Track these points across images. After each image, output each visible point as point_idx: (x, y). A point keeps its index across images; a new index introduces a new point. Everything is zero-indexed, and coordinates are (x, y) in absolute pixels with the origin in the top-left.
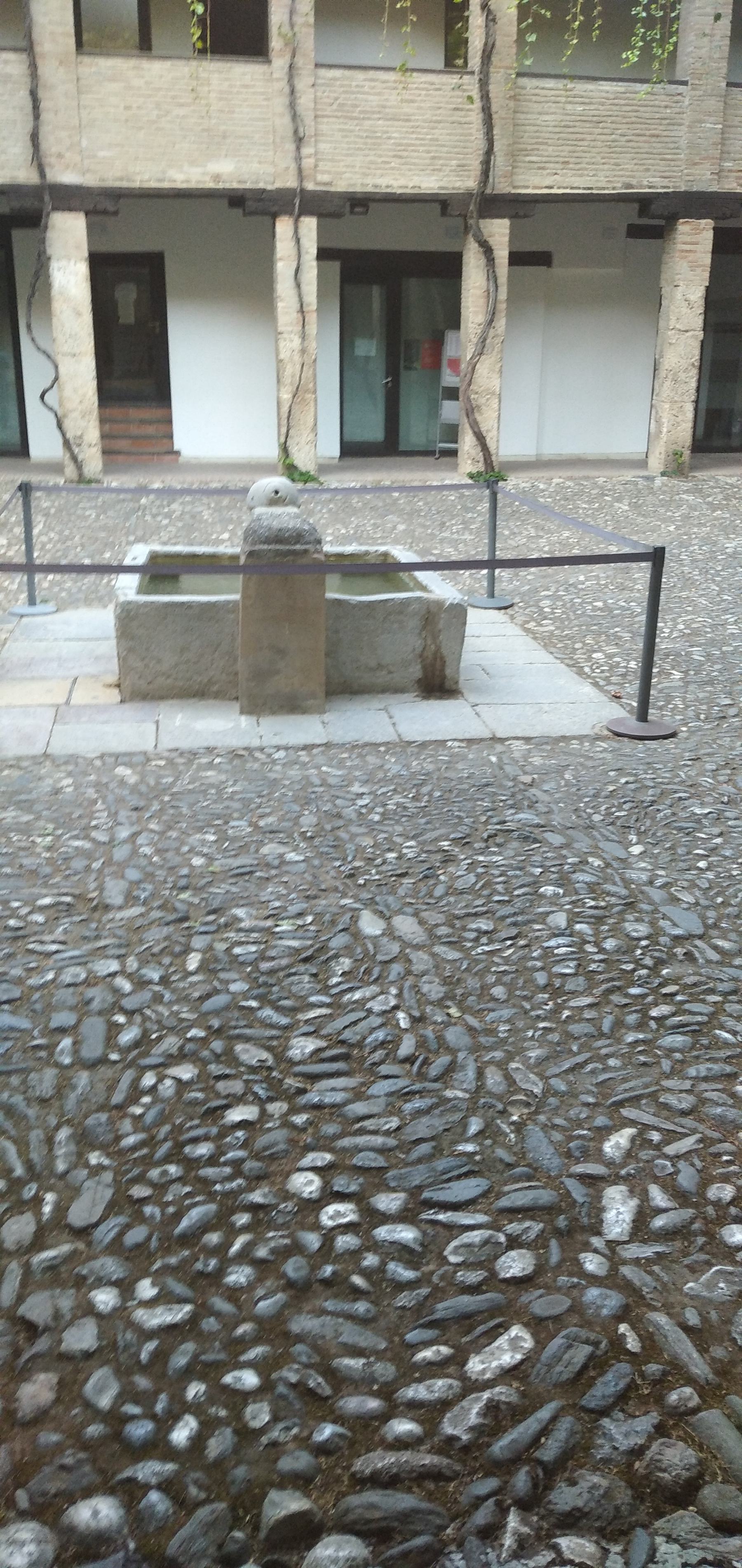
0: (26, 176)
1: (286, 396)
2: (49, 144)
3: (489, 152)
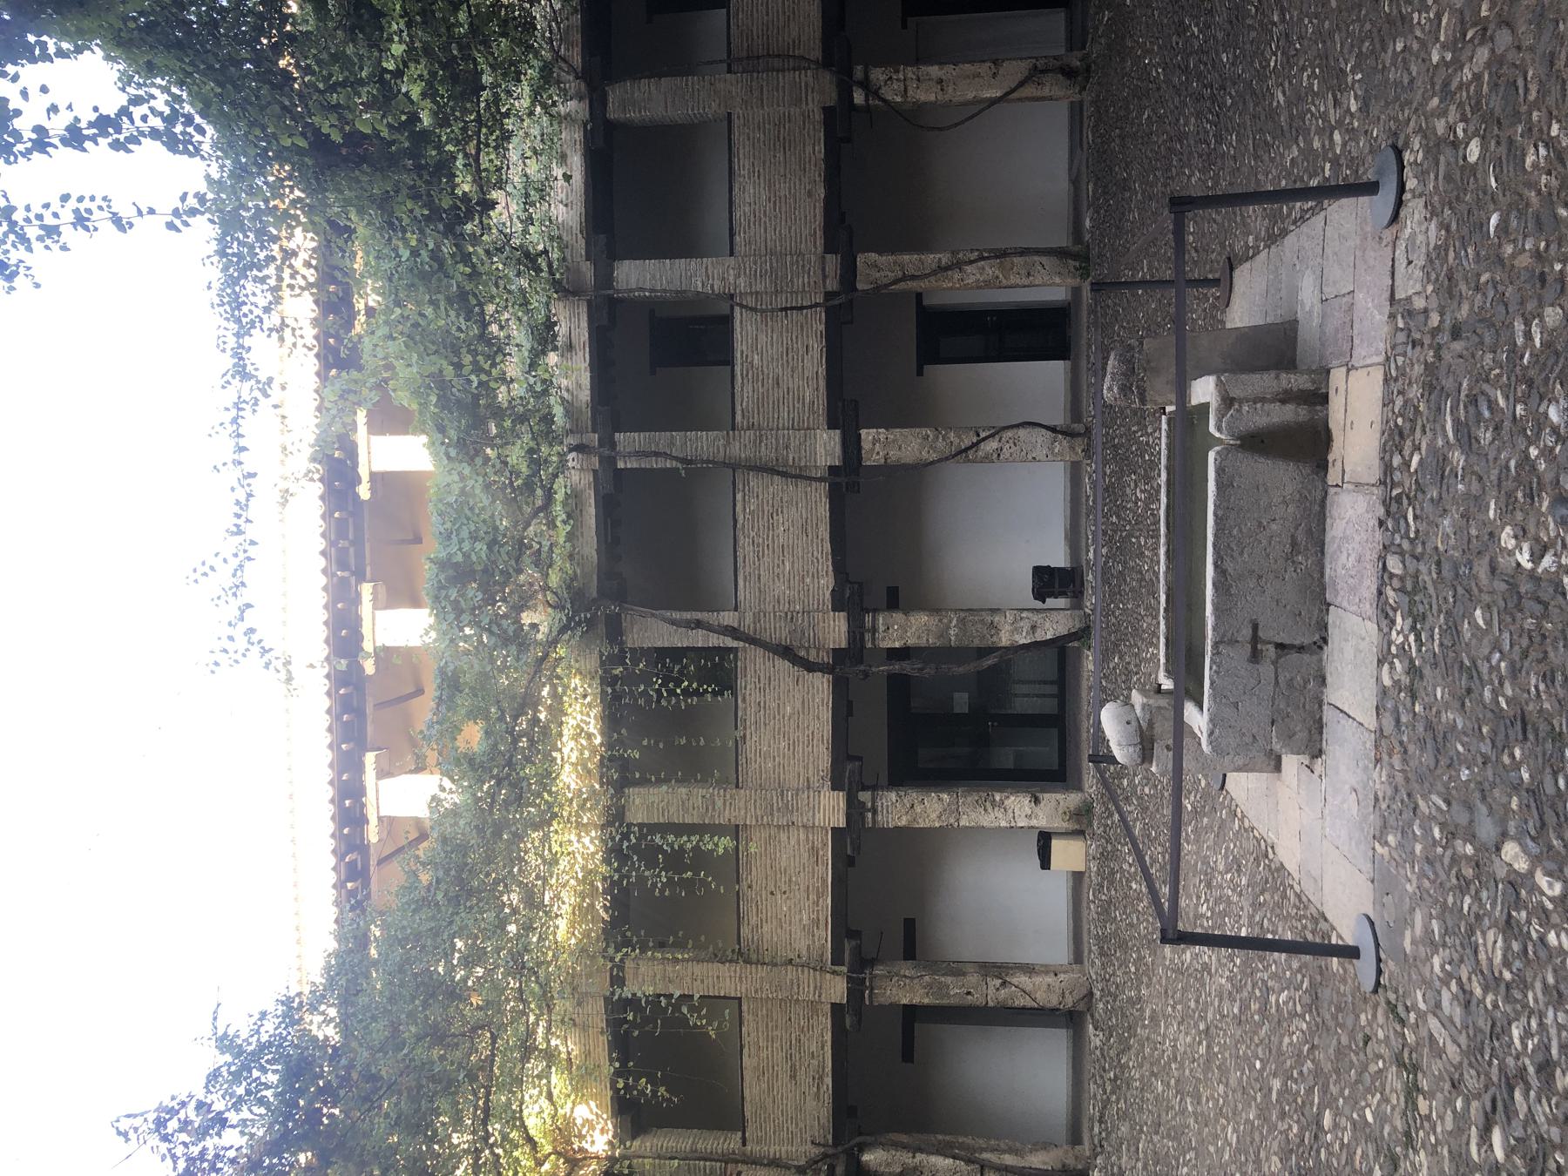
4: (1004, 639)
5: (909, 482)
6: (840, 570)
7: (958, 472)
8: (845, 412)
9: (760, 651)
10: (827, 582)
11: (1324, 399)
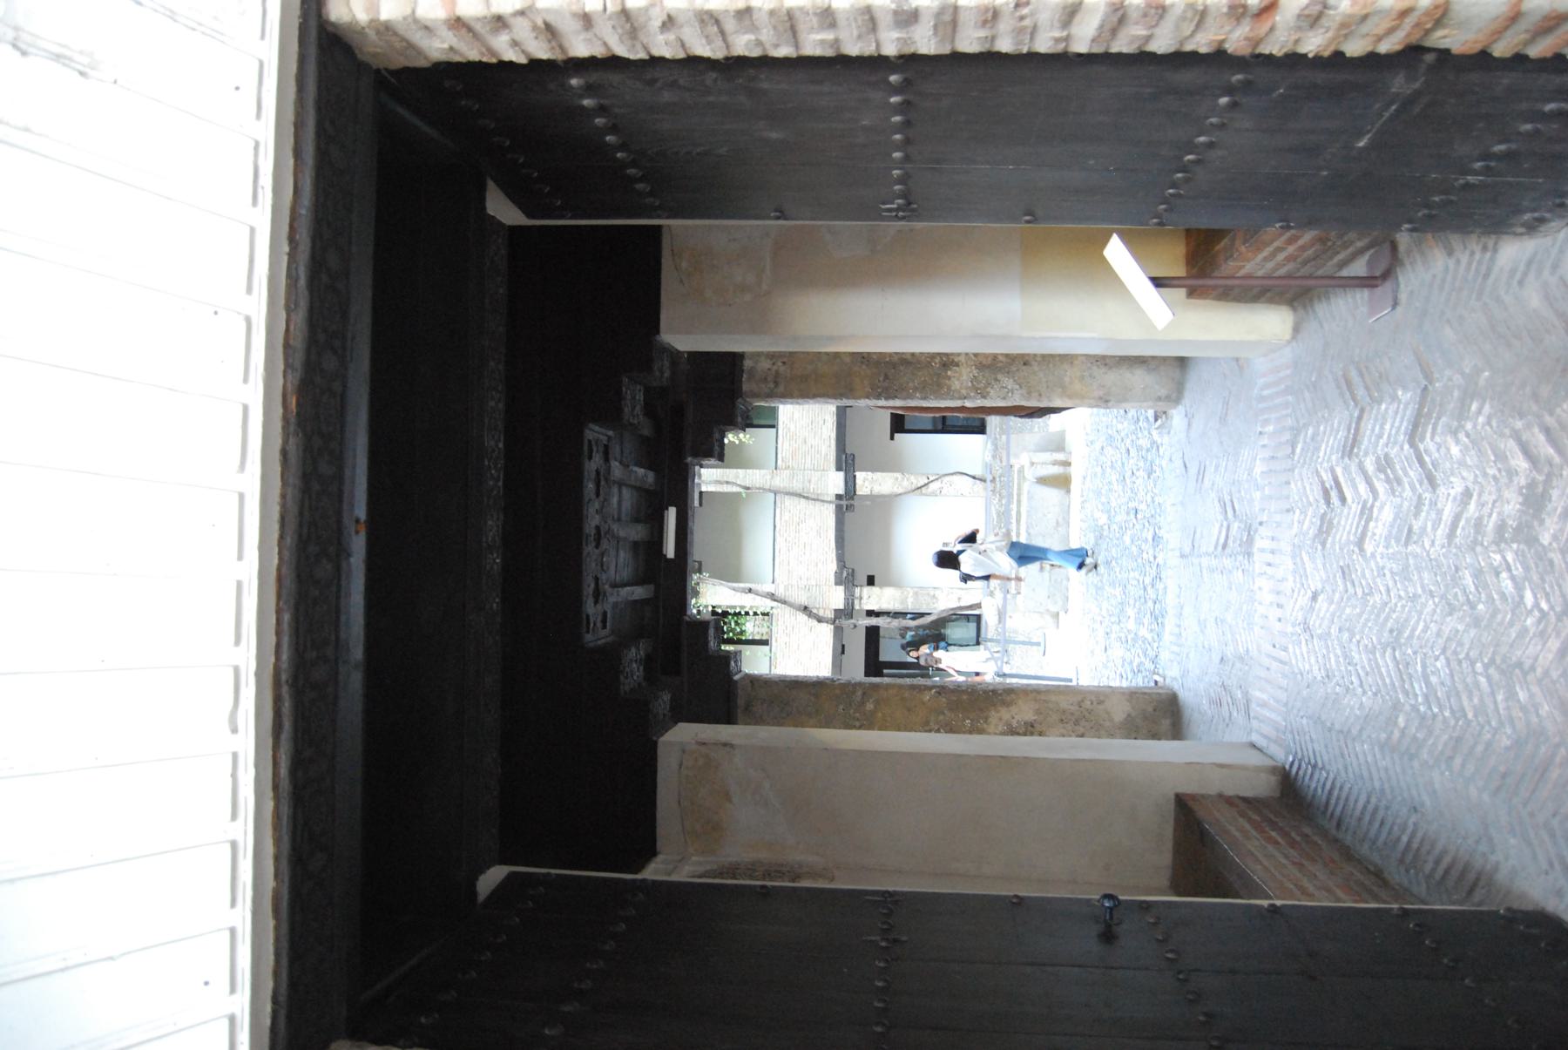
5: (884, 504)
6: (841, 559)
7: (915, 502)
8: (846, 462)
9: (787, 609)
10: (833, 566)
11: (1069, 464)
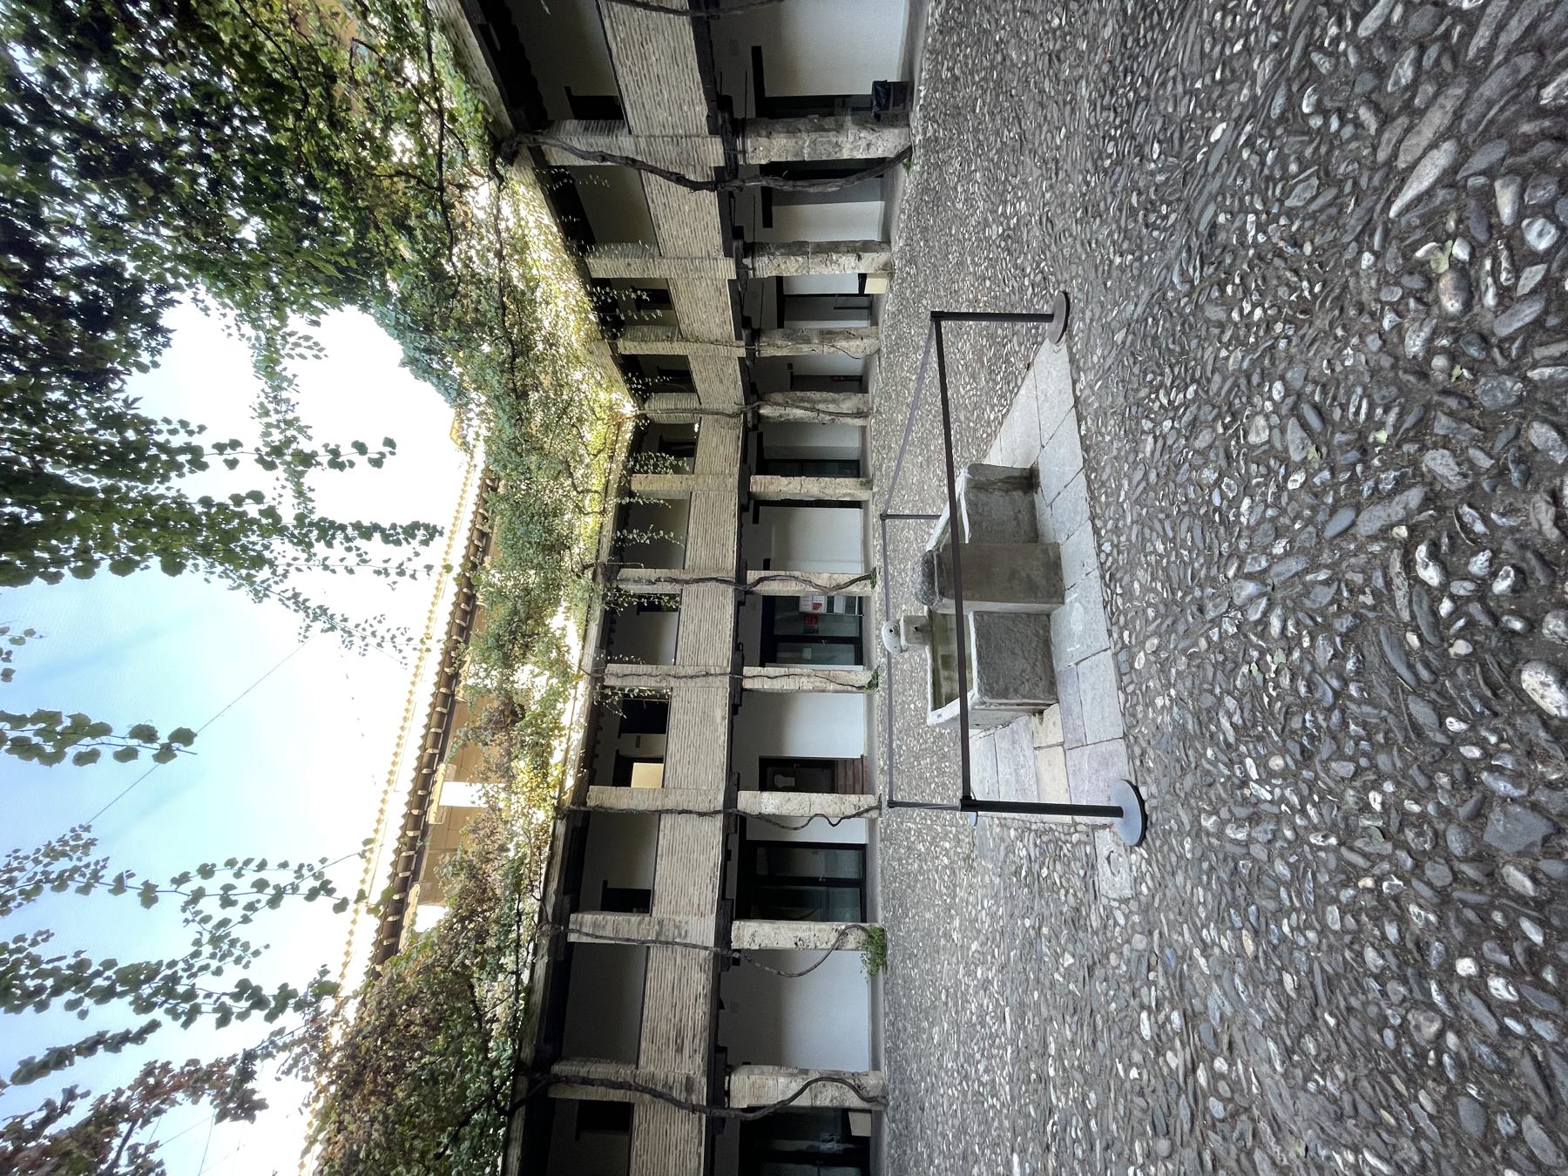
0: (719, 821)
1: (832, 687)
2: (703, 808)
3: (716, 580)
4: (846, 155)
10: (702, 110)
